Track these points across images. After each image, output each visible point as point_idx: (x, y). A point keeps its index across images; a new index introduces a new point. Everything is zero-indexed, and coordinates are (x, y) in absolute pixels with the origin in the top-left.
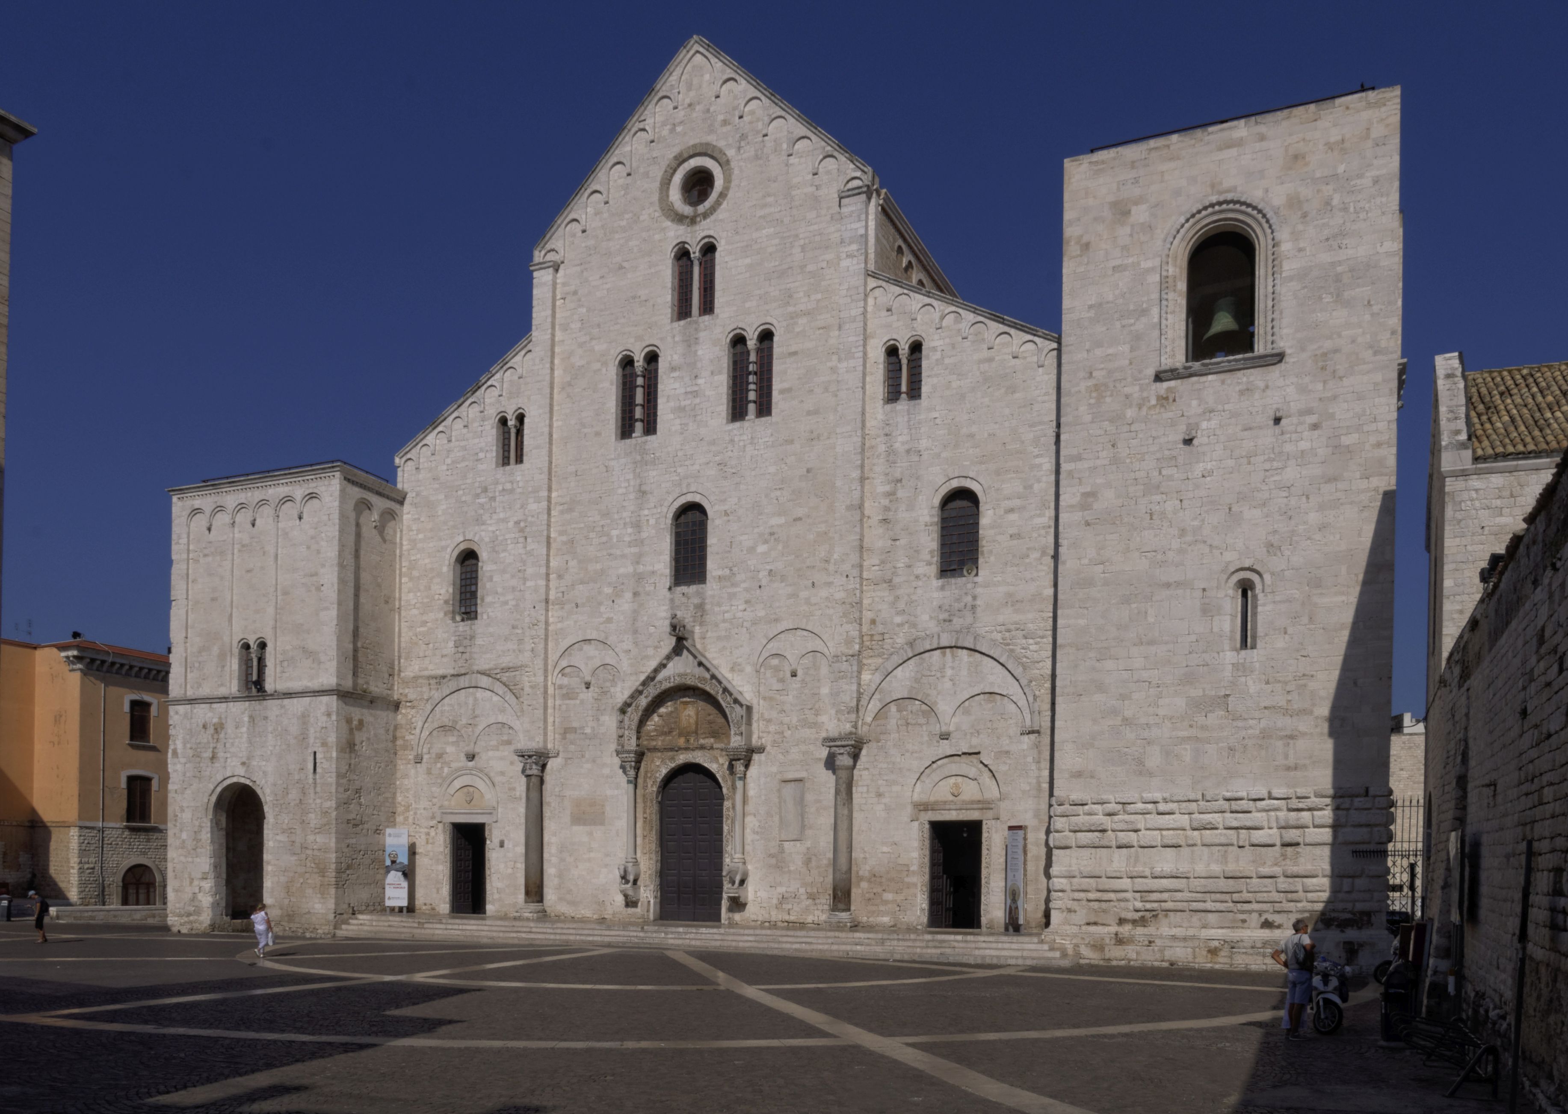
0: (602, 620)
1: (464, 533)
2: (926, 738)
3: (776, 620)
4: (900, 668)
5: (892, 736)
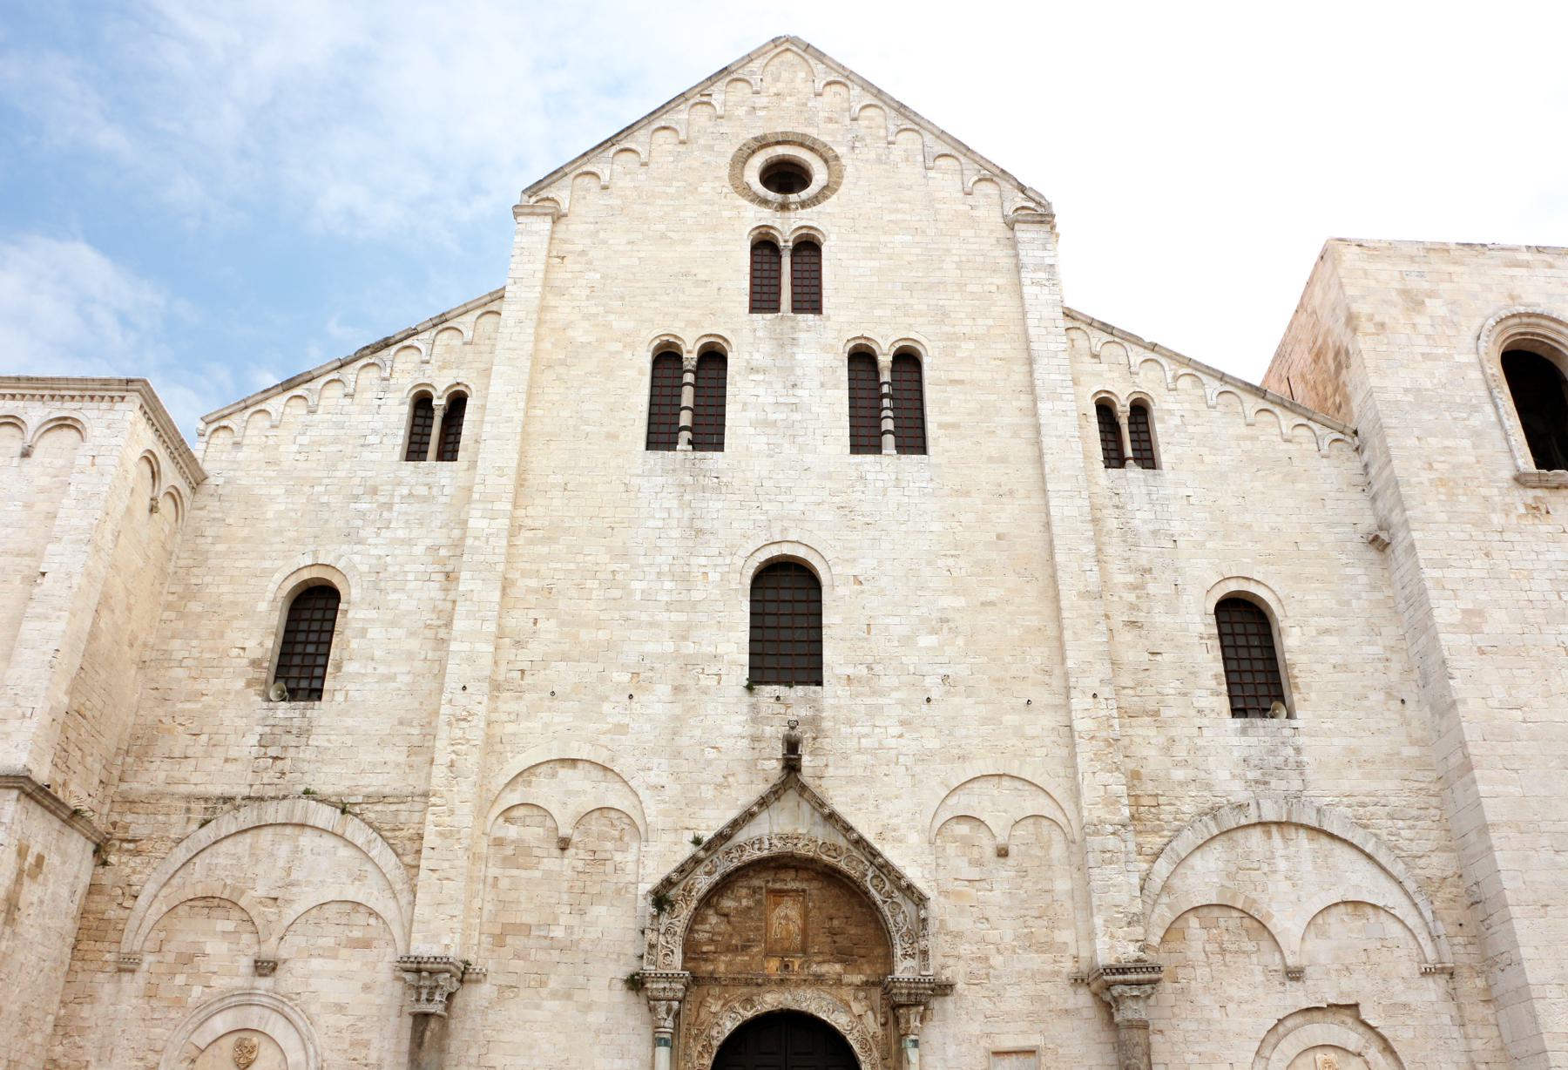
0: (606, 727)
1: (315, 552)
2: (1259, 978)
3: (962, 758)
4: (1198, 854)
5: (1199, 971)
